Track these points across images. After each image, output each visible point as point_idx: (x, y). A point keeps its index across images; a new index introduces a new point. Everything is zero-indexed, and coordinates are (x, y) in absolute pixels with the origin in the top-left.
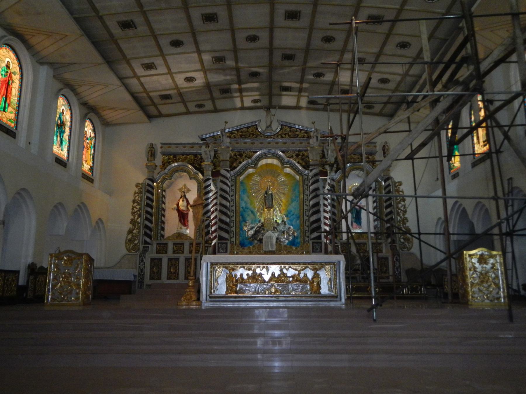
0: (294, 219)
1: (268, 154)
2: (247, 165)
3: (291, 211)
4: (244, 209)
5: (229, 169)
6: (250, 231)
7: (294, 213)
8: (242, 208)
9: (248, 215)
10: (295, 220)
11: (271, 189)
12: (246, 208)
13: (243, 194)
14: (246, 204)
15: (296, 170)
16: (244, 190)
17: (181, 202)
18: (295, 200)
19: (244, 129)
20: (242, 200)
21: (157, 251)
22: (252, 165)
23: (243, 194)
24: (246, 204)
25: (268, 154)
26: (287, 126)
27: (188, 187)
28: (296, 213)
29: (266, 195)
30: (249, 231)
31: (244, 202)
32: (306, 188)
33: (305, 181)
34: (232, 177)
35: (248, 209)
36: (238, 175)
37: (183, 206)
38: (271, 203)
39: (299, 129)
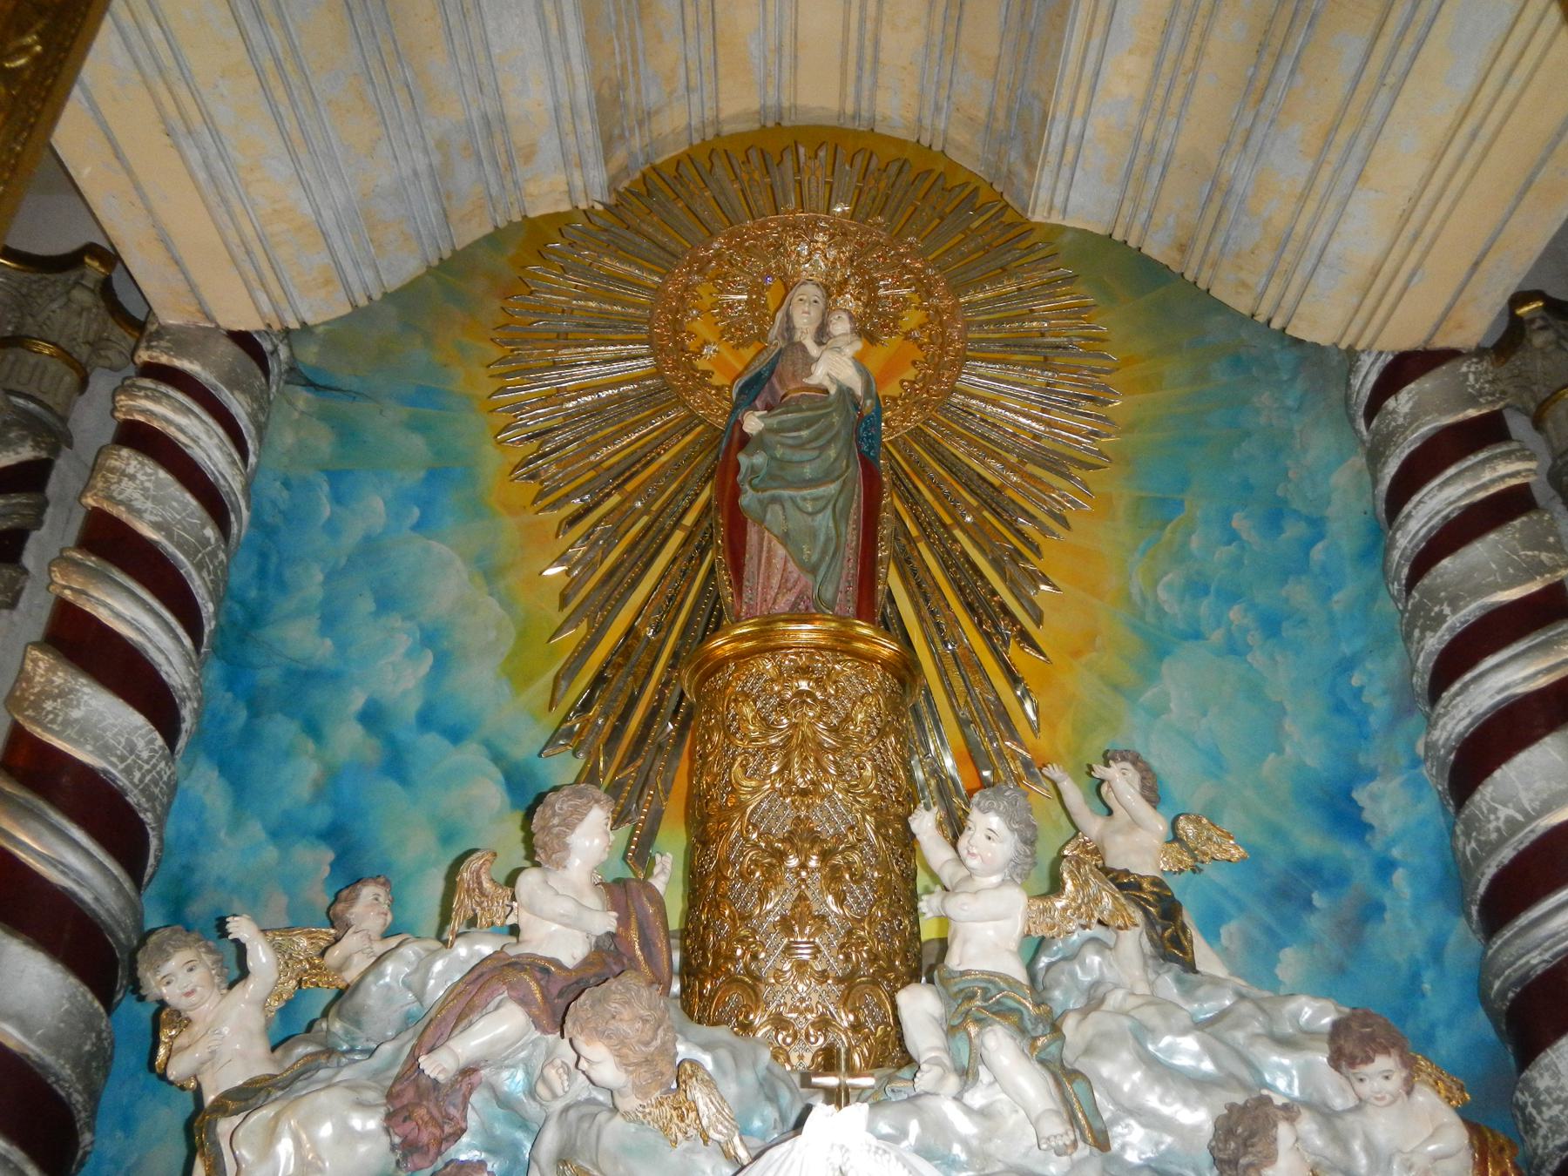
4: (391, 741)
8: (372, 717)
12: (426, 720)
13: (417, 527)
14: (442, 664)
16: (436, 476)
18: (1197, 635)
20: (386, 602)
23: (417, 527)
24: (442, 664)
35: (456, 735)
38: (852, 535)
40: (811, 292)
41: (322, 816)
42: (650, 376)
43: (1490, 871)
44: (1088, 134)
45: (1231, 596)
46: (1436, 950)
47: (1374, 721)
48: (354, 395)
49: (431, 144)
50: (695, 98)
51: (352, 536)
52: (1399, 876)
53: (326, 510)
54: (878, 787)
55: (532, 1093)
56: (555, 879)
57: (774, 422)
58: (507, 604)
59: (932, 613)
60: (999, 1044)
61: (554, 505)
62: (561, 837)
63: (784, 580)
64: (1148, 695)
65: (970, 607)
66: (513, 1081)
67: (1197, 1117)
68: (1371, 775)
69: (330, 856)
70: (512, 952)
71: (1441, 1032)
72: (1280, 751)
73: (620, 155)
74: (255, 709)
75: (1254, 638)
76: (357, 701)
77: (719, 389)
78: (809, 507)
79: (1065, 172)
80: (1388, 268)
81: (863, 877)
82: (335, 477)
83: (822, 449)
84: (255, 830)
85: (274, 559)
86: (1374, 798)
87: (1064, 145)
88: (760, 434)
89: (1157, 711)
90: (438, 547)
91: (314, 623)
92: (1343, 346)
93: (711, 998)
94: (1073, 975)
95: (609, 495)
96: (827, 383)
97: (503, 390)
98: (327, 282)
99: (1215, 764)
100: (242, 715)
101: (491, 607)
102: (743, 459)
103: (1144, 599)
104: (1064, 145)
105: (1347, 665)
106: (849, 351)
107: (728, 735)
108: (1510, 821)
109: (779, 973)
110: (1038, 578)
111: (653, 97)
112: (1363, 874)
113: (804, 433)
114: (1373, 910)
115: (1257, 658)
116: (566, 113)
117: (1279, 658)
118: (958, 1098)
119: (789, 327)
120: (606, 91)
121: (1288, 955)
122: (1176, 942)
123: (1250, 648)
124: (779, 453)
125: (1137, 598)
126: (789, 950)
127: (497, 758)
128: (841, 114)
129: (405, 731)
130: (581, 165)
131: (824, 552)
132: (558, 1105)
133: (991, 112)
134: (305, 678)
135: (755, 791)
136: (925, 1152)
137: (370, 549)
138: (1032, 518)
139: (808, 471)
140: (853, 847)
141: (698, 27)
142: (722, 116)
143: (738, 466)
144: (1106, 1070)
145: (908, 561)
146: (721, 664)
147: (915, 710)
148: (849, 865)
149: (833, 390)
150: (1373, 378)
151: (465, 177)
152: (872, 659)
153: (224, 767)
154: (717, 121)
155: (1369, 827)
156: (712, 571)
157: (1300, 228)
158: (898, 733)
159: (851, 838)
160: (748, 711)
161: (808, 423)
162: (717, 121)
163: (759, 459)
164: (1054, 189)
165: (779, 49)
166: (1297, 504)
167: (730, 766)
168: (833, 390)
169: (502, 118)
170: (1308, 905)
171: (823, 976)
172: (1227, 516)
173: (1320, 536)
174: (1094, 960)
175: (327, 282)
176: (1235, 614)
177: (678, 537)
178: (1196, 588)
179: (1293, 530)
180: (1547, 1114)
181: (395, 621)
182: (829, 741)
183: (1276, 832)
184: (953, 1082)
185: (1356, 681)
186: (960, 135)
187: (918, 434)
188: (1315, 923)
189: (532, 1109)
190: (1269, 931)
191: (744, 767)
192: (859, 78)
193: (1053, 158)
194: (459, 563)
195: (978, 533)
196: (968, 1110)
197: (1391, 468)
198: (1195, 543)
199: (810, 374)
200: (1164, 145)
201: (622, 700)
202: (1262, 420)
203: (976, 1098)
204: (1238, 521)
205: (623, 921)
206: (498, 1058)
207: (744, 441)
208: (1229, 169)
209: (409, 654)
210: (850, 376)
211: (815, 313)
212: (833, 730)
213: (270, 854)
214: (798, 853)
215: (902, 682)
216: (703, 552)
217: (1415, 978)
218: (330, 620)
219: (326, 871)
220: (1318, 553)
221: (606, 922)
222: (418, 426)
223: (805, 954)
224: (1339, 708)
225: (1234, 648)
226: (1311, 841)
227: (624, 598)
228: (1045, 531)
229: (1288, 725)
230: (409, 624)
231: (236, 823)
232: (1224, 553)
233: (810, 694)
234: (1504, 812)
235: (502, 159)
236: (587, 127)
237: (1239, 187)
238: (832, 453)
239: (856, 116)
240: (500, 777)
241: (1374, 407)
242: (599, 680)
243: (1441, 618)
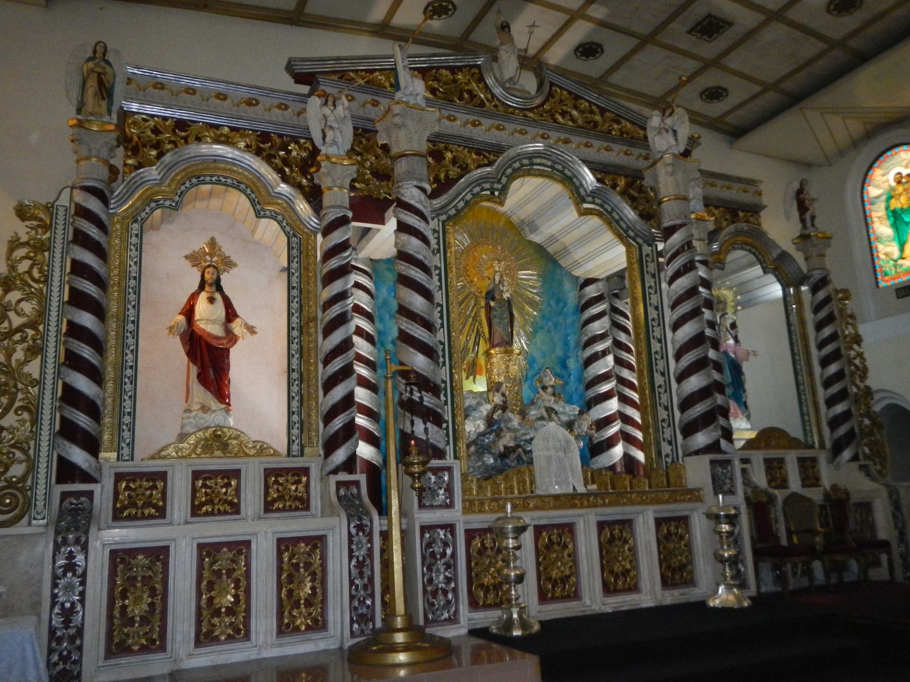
17: (202, 306)
18: (543, 328)
19: (444, 71)
21: (115, 509)
25: (538, 161)
26: (566, 90)
27: (223, 249)
29: (492, 304)
32: (653, 284)
37: (214, 322)
39: (598, 106)
45: (549, 319)
52: (572, 377)
64: (534, 341)
68: (569, 357)
75: (552, 329)
99: (544, 356)
112: (566, 377)
115: (553, 333)
173: (565, 306)
176: (549, 323)
179: (561, 305)
185: (569, 338)
210: (509, 296)
220: (565, 310)
225: (549, 331)
229: (558, 348)
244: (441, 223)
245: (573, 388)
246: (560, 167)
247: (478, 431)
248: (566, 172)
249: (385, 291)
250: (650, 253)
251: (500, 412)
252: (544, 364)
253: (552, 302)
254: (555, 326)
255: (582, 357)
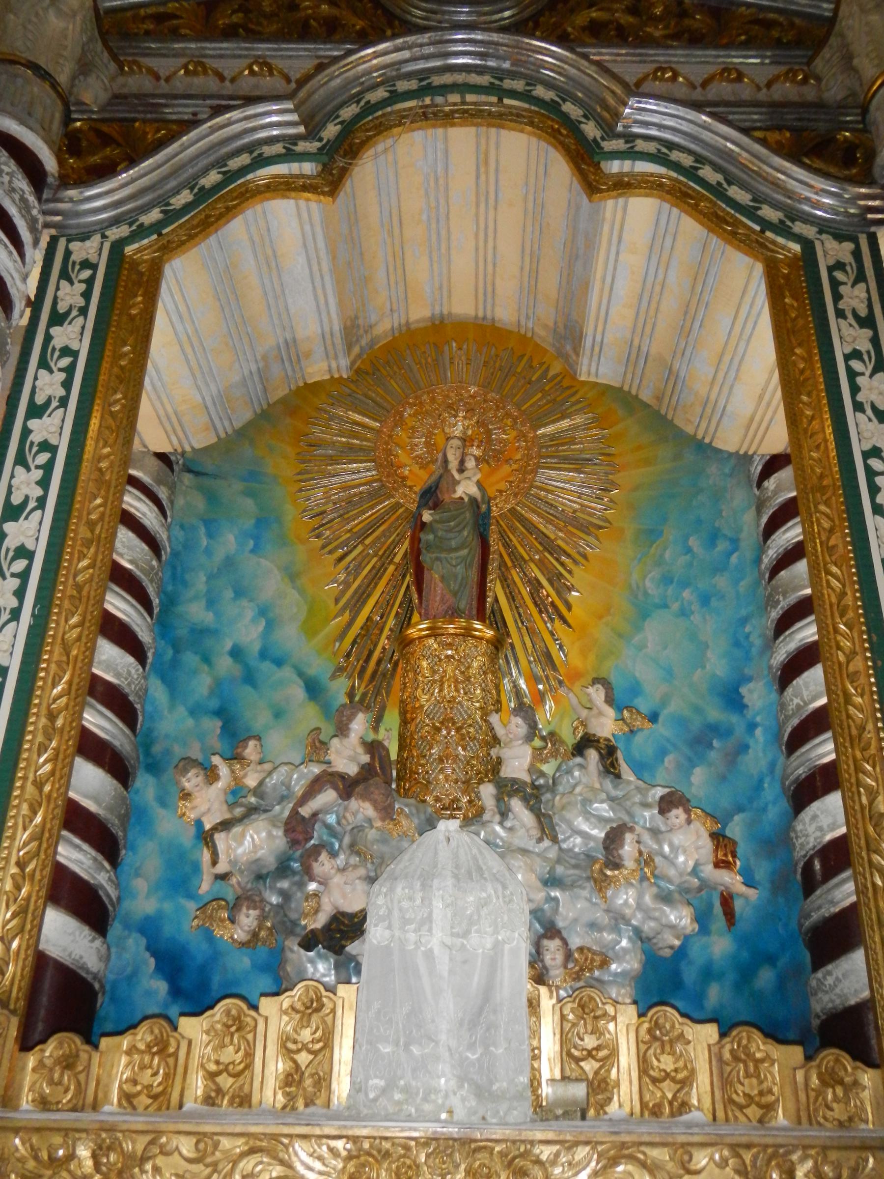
0: (662, 753)
1: (447, 79)
2: (244, 159)
3: (635, 689)
5: (50, 163)
6: (237, 830)
7: (665, 701)
8: (236, 653)
9: (278, 715)
10: (669, 760)
11: (470, 463)
12: (264, 655)
14: (270, 625)
15: (734, 192)
16: (261, 522)
18: (666, 606)
20: (240, 593)
22: (289, 156)
23: (252, 551)
24: (270, 625)
28: (674, 707)
30: (225, 825)
31: (249, 614)
33: (835, 284)
34: (75, 246)
35: (279, 663)
36: (141, 232)
38: (473, 575)
40: (456, 443)
41: (214, 704)
42: (376, 481)
43: (789, 730)
44: (605, 340)
45: (685, 584)
46: (772, 766)
47: (754, 651)
48: (215, 476)
49: (259, 357)
50: (396, 315)
51: (220, 555)
52: (759, 732)
53: (204, 542)
54: (483, 698)
55: (339, 823)
56: (346, 741)
57: (437, 517)
58: (302, 592)
59: (517, 607)
60: (516, 805)
61: (330, 552)
62: (347, 724)
63: (442, 599)
64: (637, 639)
65: (536, 604)
66: (331, 819)
67: (599, 833)
68: (750, 679)
69: (219, 724)
70: (330, 770)
71: (770, 807)
72: (704, 667)
73: (356, 350)
74: (177, 650)
75: (695, 607)
76: (228, 645)
77: (411, 488)
78: (454, 563)
79: (595, 358)
80: (757, 418)
81: (475, 738)
82: (208, 523)
83: (460, 531)
84: (181, 711)
85: (179, 569)
86: (750, 691)
87: (593, 346)
88: (431, 523)
89: (641, 647)
90: (264, 562)
91: (203, 603)
92: (742, 452)
93: (409, 789)
94: (568, 781)
95: (355, 547)
96: (464, 496)
97: (301, 490)
98: (207, 429)
99: (669, 674)
100: (170, 653)
101: (293, 595)
102: (422, 536)
103: (638, 587)
104: (593, 346)
105: (744, 621)
106: (475, 479)
107: (416, 673)
108: (798, 705)
109: (436, 779)
110: (570, 589)
111: (373, 318)
113: (452, 524)
114: (744, 748)
115: (696, 618)
116: (328, 336)
117: (708, 617)
118: (501, 823)
119: (446, 461)
120: (349, 323)
121: (698, 771)
122: (612, 765)
123: (693, 613)
124: (440, 533)
125: (634, 586)
126: (442, 770)
127: (301, 674)
128: (476, 317)
129: (253, 662)
130: (336, 357)
131: (461, 585)
132: (349, 828)
133: (555, 323)
134: (201, 633)
135: (427, 701)
136: (487, 842)
137: (229, 563)
138: (569, 556)
139: (453, 544)
140: (470, 725)
141: (397, 283)
142: (411, 320)
143: (420, 540)
144: (568, 815)
145: (506, 580)
146: (412, 641)
147: (506, 656)
148: (469, 733)
149: (466, 499)
150: (760, 468)
151: (276, 370)
152: (481, 638)
153: (163, 679)
154: (407, 324)
155: (745, 706)
156: (408, 587)
157: (713, 397)
158: (493, 673)
159: (470, 722)
160: (424, 664)
161: (454, 518)
162: (407, 324)
163: (431, 537)
164: (590, 365)
165: (441, 288)
166: (726, 531)
167: (416, 689)
168: (466, 499)
169: (294, 340)
170: (710, 746)
171: (456, 782)
172: (686, 538)
173: (736, 549)
174: (577, 774)
175: (207, 429)
176: (686, 594)
177: (391, 568)
178: (667, 580)
179: (722, 546)
180: (800, 841)
181: (244, 602)
182: (461, 678)
183: (698, 710)
184: (497, 818)
185: (748, 629)
186: (542, 333)
187: (512, 511)
188: (713, 755)
189: (338, 829)
190: (690, 760)
191: (423, 690)
192: (485, 301)
193: (588, 352)
194: (276, 571)
195: (542, 565)
196: (503, 827)
197: (765, 519)
198: (667, 555)
199: (455, 491)
200: (644, 349)
201: (366, 653)
202: (711, 482)
203: (508, 824)
204: (693, 542)
205: (373, 758)
206: (326, 810)
207: (423, 525)
208: (676, 365)
209: (254, 620)
210: (474, 490)
211: (459, 453)
212: (462, 673)
213: (190, 722)
214: (447, 728)
215: (497, 648)
216: (404, 577)
217: (761, 781)
218: (211, 603)
219: (218, 731)
220: (734, 559)
221: (366, 759)
222: (249, 493)
223: (449, 771)
224: (737, 644)
225: (684, 613)
226: (715, 714)
227: (364, 603)
228: (575, 562)
229: (709, 654)
230: (252, 604)
231: (172, 707)
232: (684, 559)
233: (452, 657)
234: (796, 701)
235: (294, 358)
236: (338, 340)
237: (682, 374)
238: (465, 533)
239: (484, 318)
240: (302, 684)
241: (759, 485)
242: (354, 642)
243: (778, 602)
244: (107, 246)
245: (763, 764)
246: (519, 85)
247: (807, 923)
248: (540, 91)
249: (231, 538)
250: (848, 259)
251: (328, 796)
252: (665, 701)
253: (693, 542)
254: (705, 600)
255: (770, 667)
